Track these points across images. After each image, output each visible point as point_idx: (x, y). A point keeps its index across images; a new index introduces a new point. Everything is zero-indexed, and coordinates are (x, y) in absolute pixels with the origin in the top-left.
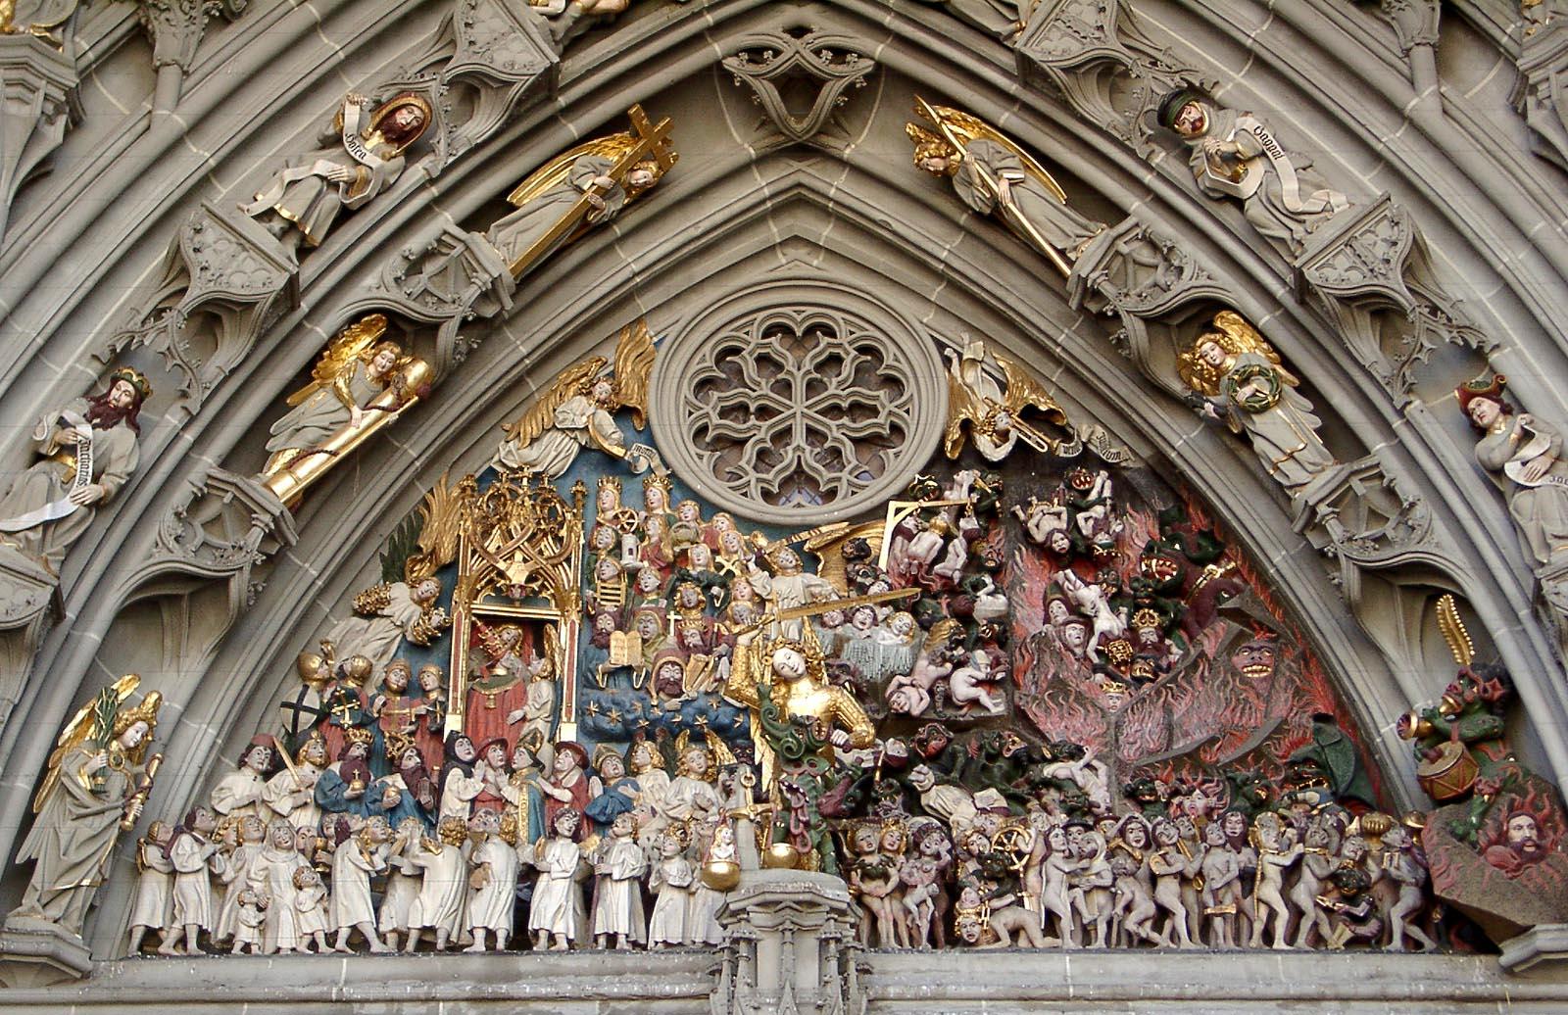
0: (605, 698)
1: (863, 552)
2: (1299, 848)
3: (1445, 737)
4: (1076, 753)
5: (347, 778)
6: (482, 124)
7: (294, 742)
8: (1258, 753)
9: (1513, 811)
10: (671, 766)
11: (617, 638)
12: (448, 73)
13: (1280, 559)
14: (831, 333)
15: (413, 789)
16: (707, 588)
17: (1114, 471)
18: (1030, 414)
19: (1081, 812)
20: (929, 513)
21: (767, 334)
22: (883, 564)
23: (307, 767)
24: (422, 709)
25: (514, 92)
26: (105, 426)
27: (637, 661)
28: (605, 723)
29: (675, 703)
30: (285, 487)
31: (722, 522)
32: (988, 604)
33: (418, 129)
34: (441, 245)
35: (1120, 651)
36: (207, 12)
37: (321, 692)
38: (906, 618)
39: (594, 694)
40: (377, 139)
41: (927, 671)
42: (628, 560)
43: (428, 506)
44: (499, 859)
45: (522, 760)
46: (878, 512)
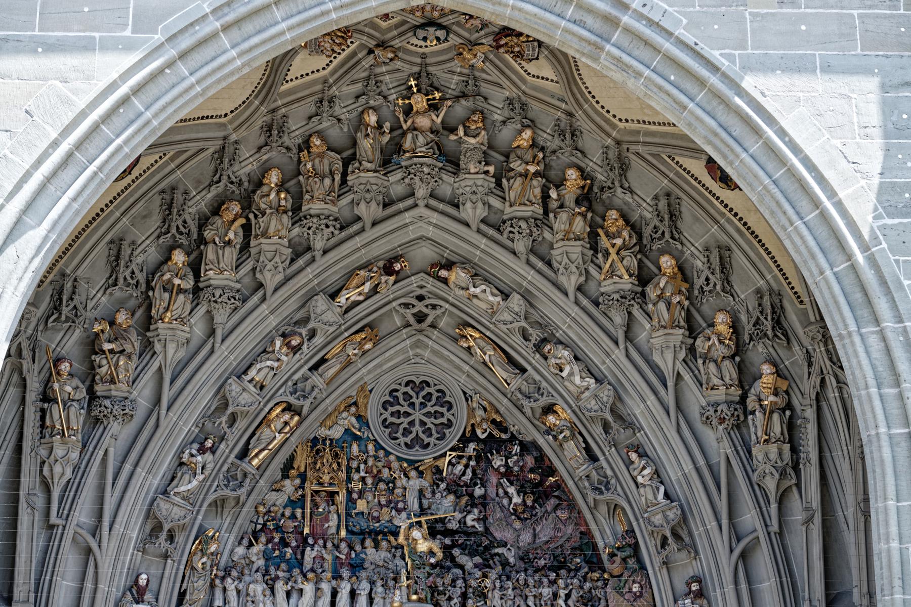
0: (355, 521)
1: (439, 471)
2: (571, 587)
3: (616, 555)
4: (505, 545)
5: (274, 550)
6: (318, 340)
7: (256, 535)
8: (562, 546)
9: (634, 582)
10: (377, 546)
11: (359, 502)
13: (570, 483)
14: (428, 385)
15: (295, 554)
16: (387, 485)
17: (522, 444)
18: (494, 422)
19: (505, 563)
20: (460, 457)
21: (407, 384)
22: (444, 475)
23: (261, 545)
24: (296, 524)
26: (204, 453)
27: (366, 511)
28: (354, 529)
29: (377, 525)
30: (255, 462)
31: (392, 458)
32: (478, 492)
34: (305, 379)
35: (520, 509)
37: (263, 517)
38: (451, 497)
39: (352, 520)
40: (285, 350)
41: (458, 516)
42: (362, 474)
43: (295, 451)
44: (326, 587)
45: (329, 545)
46: (444, 455)
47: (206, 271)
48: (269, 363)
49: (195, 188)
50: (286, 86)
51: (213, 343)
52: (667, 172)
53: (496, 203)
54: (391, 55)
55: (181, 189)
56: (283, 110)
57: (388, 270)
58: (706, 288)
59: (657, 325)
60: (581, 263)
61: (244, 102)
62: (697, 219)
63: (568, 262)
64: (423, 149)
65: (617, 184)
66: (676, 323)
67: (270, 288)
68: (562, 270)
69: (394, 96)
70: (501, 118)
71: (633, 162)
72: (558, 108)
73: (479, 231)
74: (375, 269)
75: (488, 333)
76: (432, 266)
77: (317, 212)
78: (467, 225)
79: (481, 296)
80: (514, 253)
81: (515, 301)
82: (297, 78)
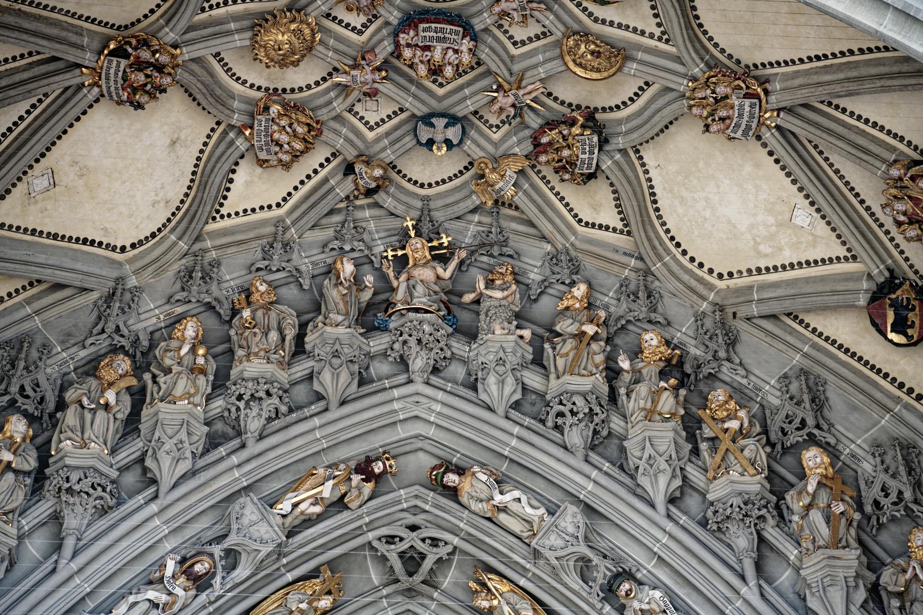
6: (241, 572)
12: (226, 544)
25: (261, 556)
33: (207, 573)
36: (95, 507)
40: (182, 580)
47: (60, 441)
48: (151, 594)
49: (62, 342)
50: (221, 224)
51: (56, 561)
52: (799, 345)
53: (533, 379)
54: (378, 172)
55: (39, 341)
56: (214, 254)
57: (364, 468)
58: (883, 501)
59: (811, 547)
60: (674, 456)
61: (153, 235)
62: (855, 408)
63: (653, 453)
64: (424, 300)
65: (722, 354)
66: (844, 543)
67: (166, 481)
68: (642, 464)
69: (382, 248)
70: (539, 278)
71: (744, 337)
72: (624, 266)
73: (507, 417)
74: (342, 466)
75: (522, 582)
76: (433, 469)
77: (254, 375)
78: (490, 409)
79: (514, 507)
80: (566, 448)
81: (569, 519)
82: (237, 214)
